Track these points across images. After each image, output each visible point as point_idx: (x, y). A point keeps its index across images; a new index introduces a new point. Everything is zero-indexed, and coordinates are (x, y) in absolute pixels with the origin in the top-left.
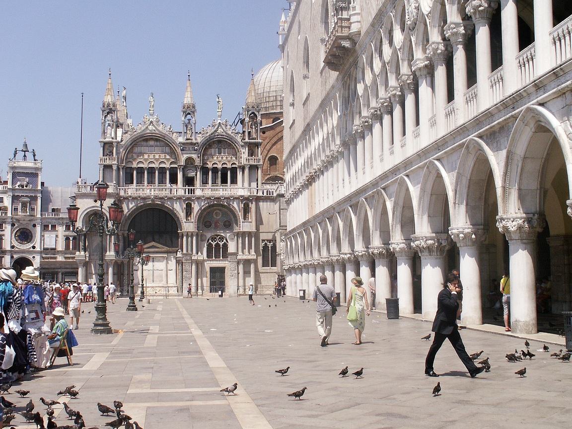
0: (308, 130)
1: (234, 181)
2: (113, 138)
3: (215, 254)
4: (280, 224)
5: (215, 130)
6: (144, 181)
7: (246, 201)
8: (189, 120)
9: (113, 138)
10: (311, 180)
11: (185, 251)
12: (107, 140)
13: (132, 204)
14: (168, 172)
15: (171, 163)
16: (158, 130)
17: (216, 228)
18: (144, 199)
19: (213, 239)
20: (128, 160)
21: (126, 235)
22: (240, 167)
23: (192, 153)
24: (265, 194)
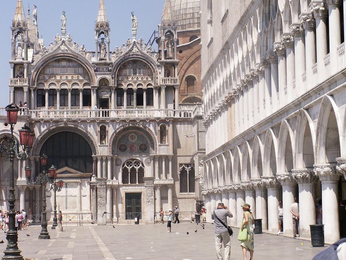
0: (227, 49)
1: (150, 102)
2: (23, 59)
3: (130, 179)
4: (198, 147)
5: (129, 49)
6: (56, 104)
7: (163, 124)
8: (103, 39)
9: (23, 59)
10: (230, 102)
11: (99, 176)
12: (18, 60)
13: (44, 127)
14: (81, 94)
15: (84, 85)
16: (71, 50)
17: (132, 151)
18: (56, 122)
19: (129, 163)
20: (40, 82)
21: (38, 160)
22: (156, 88)
23: (106, 74)
24: (182, 116)
